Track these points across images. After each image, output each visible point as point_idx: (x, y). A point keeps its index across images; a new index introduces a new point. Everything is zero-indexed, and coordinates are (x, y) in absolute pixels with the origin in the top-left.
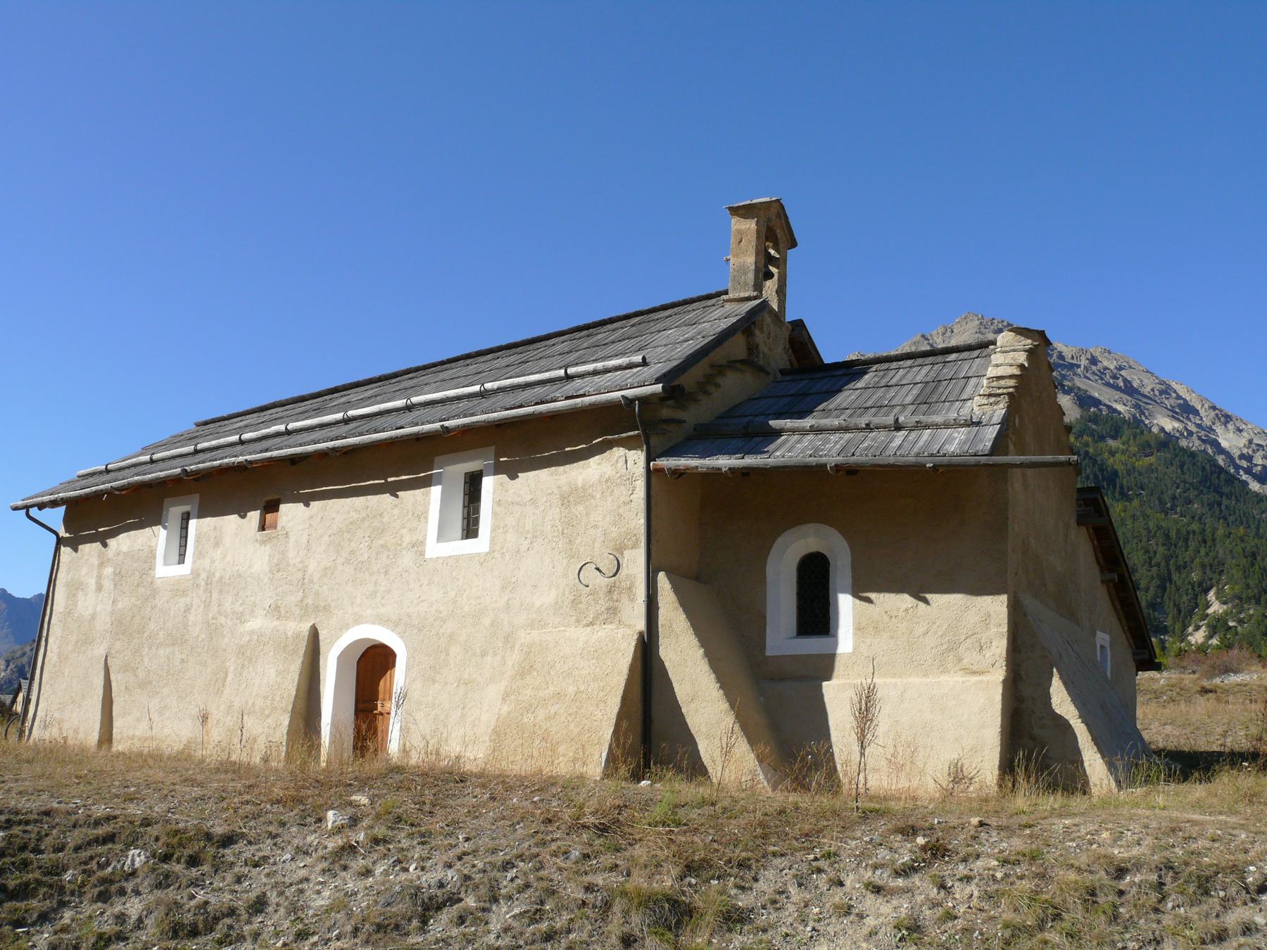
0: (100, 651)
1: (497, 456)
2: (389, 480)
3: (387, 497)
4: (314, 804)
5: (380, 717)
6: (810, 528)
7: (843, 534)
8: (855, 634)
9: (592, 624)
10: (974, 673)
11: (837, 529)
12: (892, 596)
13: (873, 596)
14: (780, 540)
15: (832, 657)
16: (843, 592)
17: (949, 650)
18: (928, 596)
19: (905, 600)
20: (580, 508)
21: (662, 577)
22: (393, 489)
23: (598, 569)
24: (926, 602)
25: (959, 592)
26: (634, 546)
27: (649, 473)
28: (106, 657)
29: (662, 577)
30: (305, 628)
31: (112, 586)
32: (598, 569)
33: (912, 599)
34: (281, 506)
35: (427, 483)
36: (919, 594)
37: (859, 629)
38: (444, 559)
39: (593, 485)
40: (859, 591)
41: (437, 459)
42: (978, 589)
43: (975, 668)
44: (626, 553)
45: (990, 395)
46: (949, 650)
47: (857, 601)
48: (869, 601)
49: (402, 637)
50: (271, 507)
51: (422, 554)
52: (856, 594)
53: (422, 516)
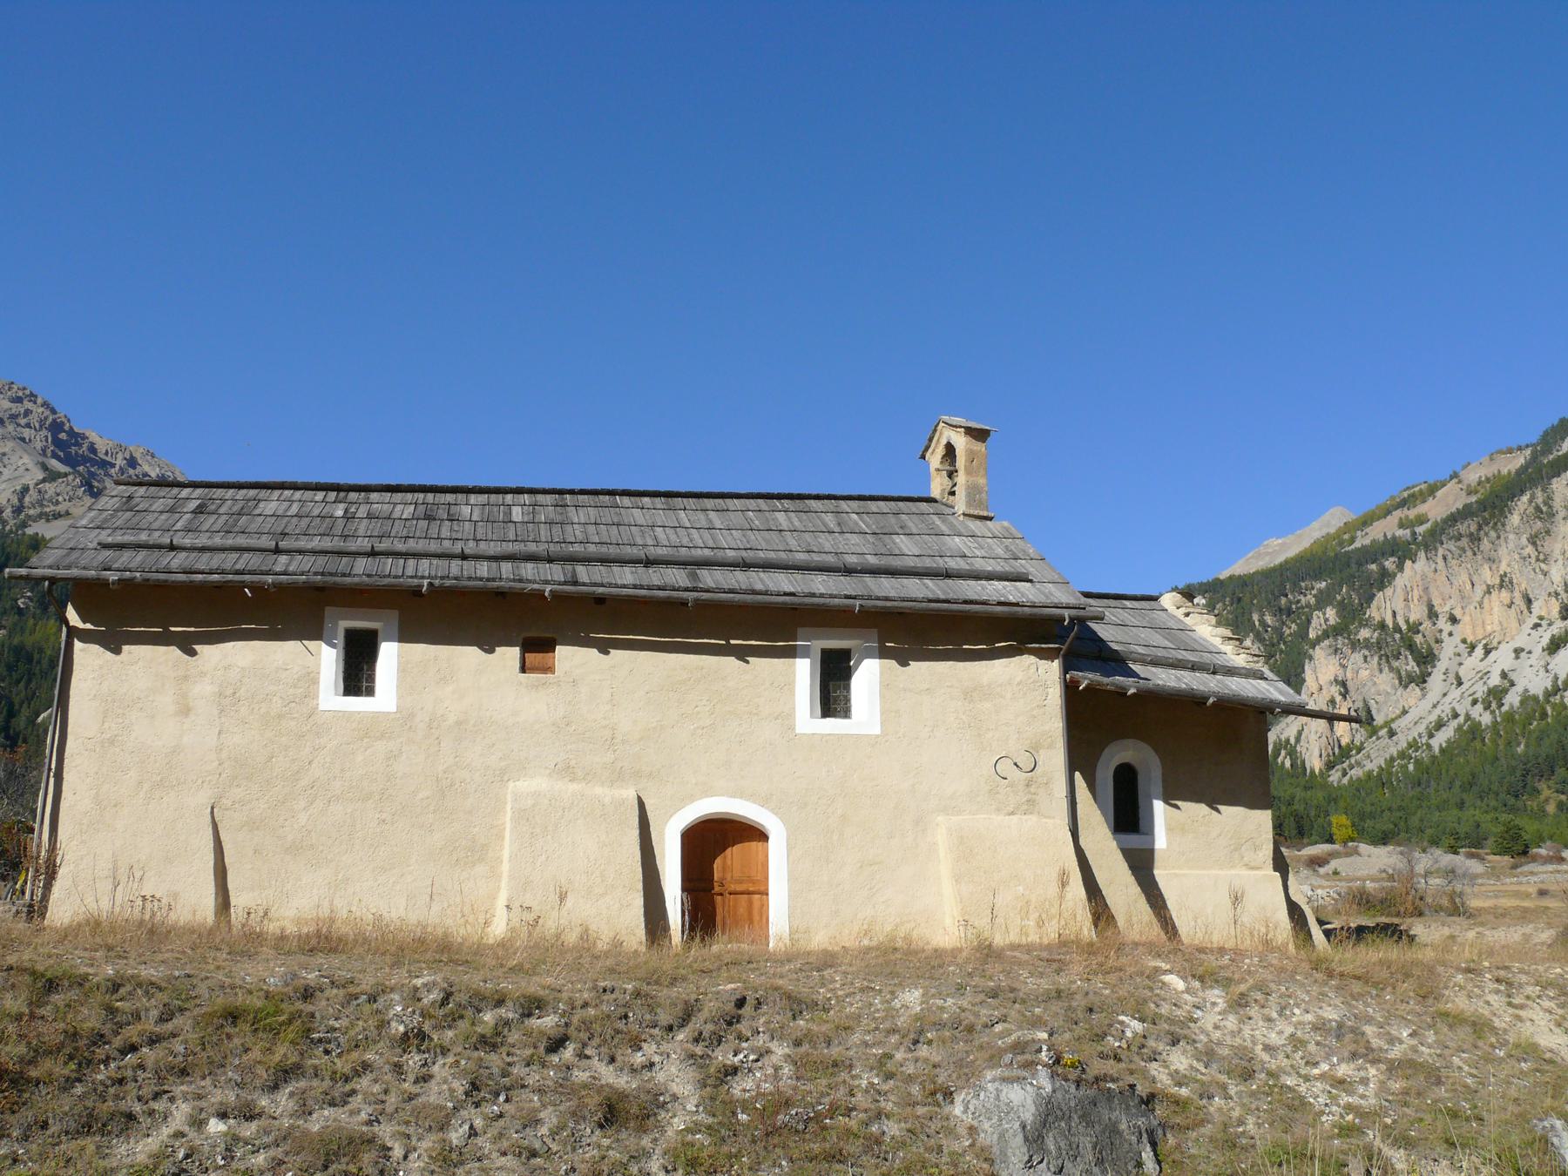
0: (203, 798)
1: (882, 641)
2: (732, 642)
3: (731, 661)
4: (1306, 966)
5: (719, 897)
6: (1129, 742)
7: (1156, 751)
8: (1167, 834)
9: (1012, 813)
10: (1252, 868)
11: (1150, 745)
12: (1193, 804)
13: (1179, 803)
14: (1106, 751)
15: (1151, 852)
16: (1157, 799)
17: (1236, 850)
18: (1220, 807)
19: (1202, 809)
20: (987, 705)
21: (1077, 774)
22: (742, 654)
23: (1015, 764)
24: (1218, 811)
25: (1240, 805)
26: (1051, 746)
27: (1070, 689)
28: (212, 808)
29: (1077, 774)
30: (630, 794)
31: (216, 712)
32: (1015, 764)
33: (1207, 808)
34: (558, 648)
35: (791, 653)
36: (1213, 804)
37: (1170, 829)
38: (823, 736)
39: (1001, 685)
40: (1168, 799)
41: (800, 631)
42: (1252, 805)
43: (1252, 864)
44: (1041, 752)
45: (1255, 655)
46: (1236, 850)
47: (1167, 806)
48: (1177, 807)
49: (776, 814)
50: (547, 646)
51: (792, 728)
52: (1166, 802)
53: (789, 686)
